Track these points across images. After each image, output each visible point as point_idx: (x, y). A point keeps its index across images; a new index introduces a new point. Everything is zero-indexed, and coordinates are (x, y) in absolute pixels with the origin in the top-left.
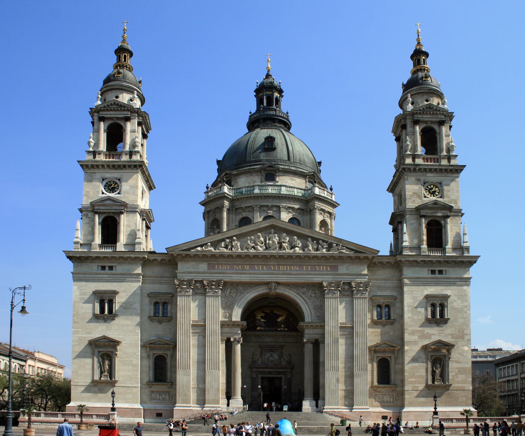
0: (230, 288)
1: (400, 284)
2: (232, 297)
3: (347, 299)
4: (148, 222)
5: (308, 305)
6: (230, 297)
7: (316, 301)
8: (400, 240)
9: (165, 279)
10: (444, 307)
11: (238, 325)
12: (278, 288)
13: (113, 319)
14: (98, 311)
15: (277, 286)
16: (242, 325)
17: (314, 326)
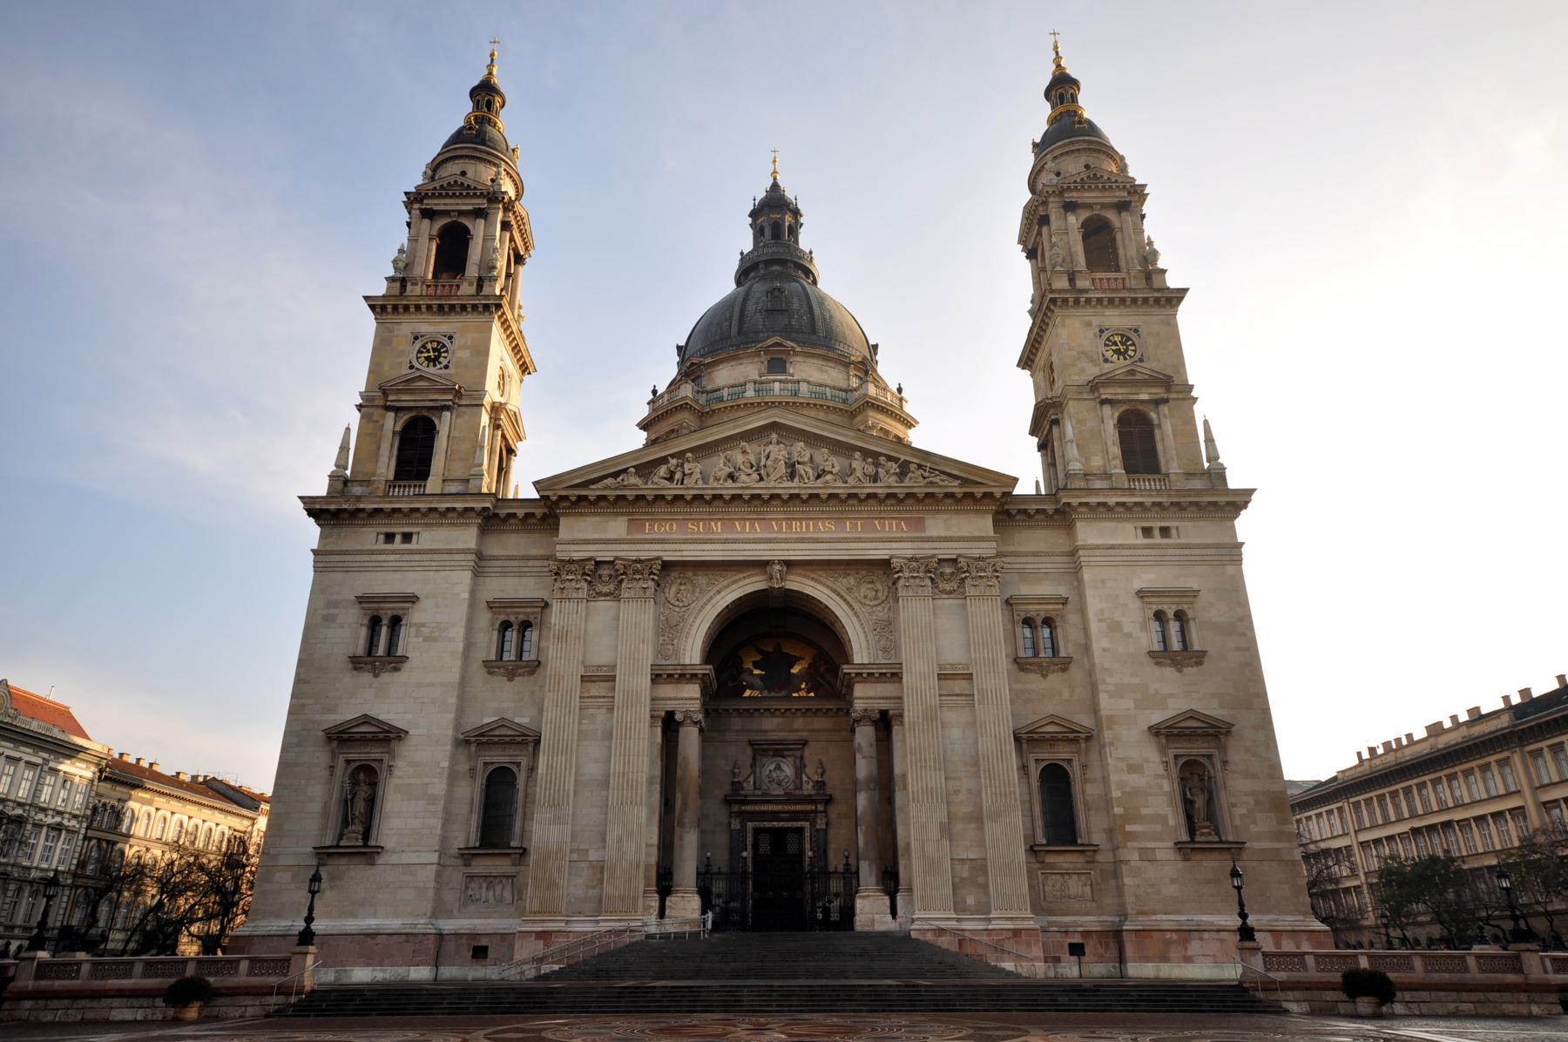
0: (679, 581)
1: (1072, 565)
2: (681, 604)
3: (951, 601)
4: (508, 436)
5: (860, 620)
6: (677, 603)
7: (879, 608)
8: (1059, 461)
9: (531, 563)
10: (1188, 621)
11: (694, 676)
12: (790, 577)
13: (396, 669)
14: (360, 650)
15: (787, 573)
16: (704, 674)
17: (877, 675)
